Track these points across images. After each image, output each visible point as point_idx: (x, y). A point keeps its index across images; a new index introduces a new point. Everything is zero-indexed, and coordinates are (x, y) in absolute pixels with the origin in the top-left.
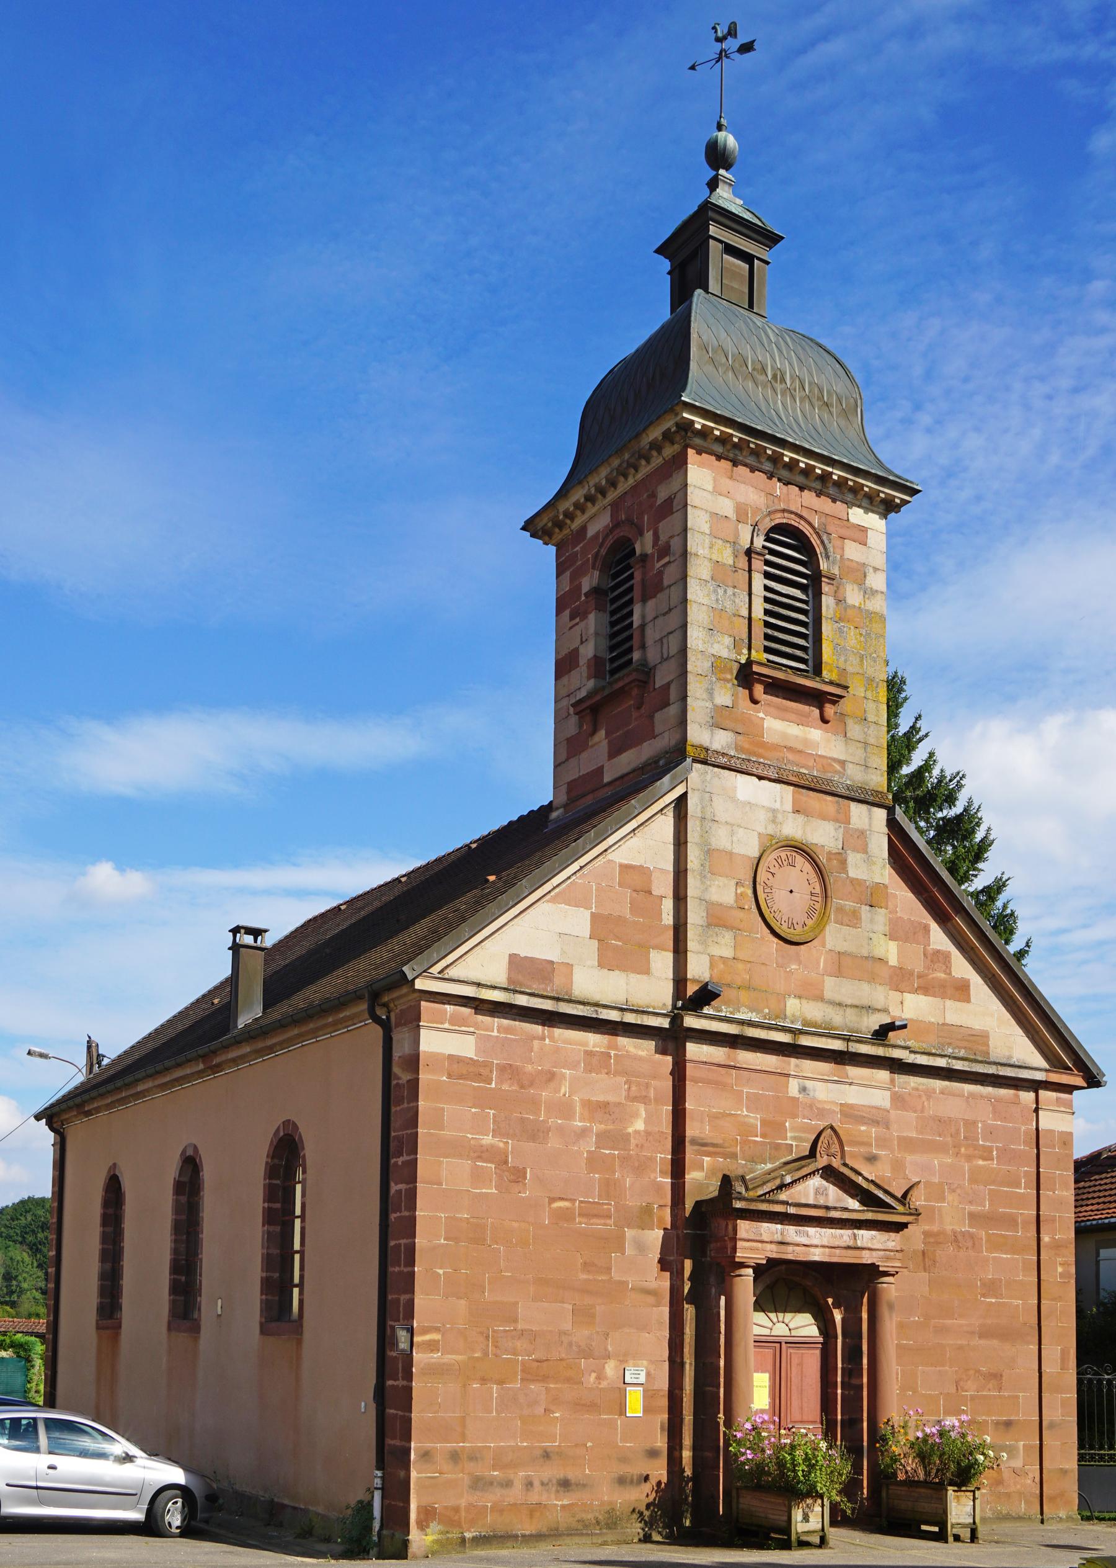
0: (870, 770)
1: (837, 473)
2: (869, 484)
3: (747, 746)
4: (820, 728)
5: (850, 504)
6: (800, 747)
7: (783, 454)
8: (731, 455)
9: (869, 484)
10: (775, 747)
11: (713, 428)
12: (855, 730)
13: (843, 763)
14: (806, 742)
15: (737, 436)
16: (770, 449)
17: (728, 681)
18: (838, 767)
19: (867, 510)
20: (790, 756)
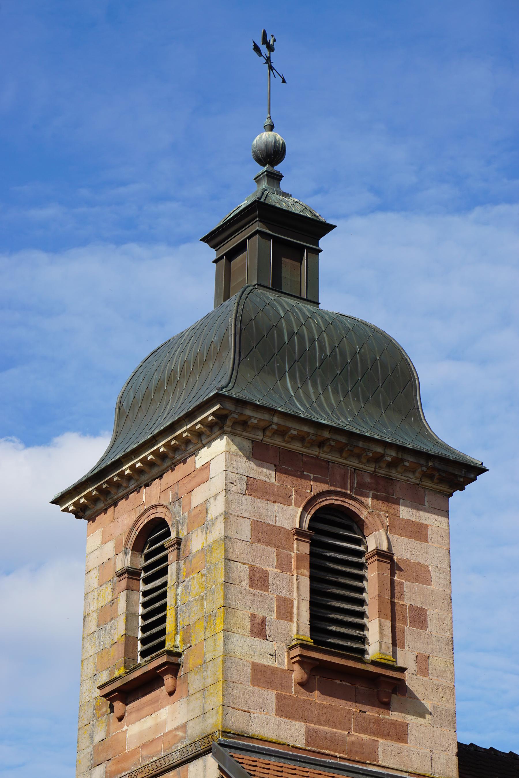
0: (208, 715)
1: (160, 446)
2: (185, 428)
3: (113, 768)
4: (168, 704)
5: (194, 454)
6: (151, 739)
7: (124, 471)
8: (110, 501)
9: (185, 428)
10: (135, 751)
11: (79, 500)
12: (195, 682)
13: (183, 727)
14: (158, 727)
15: (92, 490)
16: (114, 476)
17: (103, 715)
18: (180, 734)
19: (208, 444)
20: (144, 753)
